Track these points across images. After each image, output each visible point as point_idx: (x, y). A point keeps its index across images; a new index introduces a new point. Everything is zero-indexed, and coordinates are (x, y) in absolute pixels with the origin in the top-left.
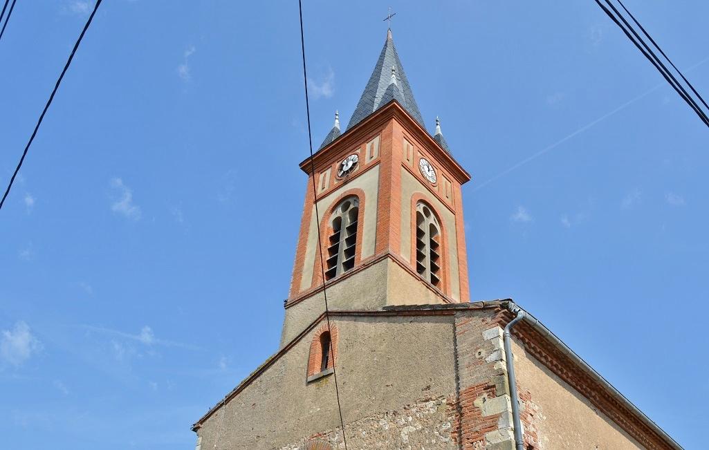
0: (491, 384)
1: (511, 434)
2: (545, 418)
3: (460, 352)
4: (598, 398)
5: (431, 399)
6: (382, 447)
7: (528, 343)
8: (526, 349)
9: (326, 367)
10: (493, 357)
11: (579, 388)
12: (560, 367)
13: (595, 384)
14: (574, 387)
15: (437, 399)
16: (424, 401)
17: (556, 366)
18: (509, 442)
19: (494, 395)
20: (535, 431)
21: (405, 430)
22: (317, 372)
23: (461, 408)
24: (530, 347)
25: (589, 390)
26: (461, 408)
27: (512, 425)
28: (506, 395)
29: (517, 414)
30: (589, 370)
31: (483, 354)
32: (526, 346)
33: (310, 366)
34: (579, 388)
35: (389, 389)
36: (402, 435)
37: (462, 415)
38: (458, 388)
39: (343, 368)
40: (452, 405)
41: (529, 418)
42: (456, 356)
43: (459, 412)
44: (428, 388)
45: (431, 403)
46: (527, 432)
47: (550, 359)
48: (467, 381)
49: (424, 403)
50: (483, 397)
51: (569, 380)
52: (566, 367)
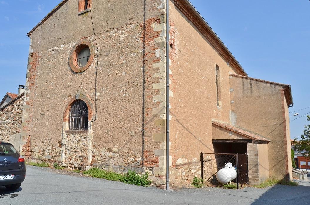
0: (159, 18)
1: (165, 39)
2: (179, 34)
3: (146, 3)
4: (201, 28)
5: (133, 23)
6: (111, 43)
7: (176, 2)
8: (175, 4)
9: (87, 8)
10: (161, 6)
11: (194, 23)
12: (188, 13)
13: (201, 22)
14: (192, 23)
15: (135, 24)
16: (130, 24)
17: (186, 13)
18: (164, 42)
19: (159, 23)
20: (174, 38)
21: (121, 36)
22: (83, 10)
23: (145, 28)
24: (177, 3)
25: (198, 24)
26: (145, 28)
27: (165, 35)
28: (164, 23)
29: (168, 32)
30: (199, 16)
31: (157, 5)
32: (175, 3)
33: (79, 7)
34: (194, 23)
35: (115, 18)
36: (120, 38)
37: (145, 30)
38: (145, 19)
39: (94, 9)
40: (142, 26)
41: (173, 33)
42: (145, 5)
43: (144, 29)
44: (132, 18)
45: (133, 25)
46: (171, 39)
47: (184, 10)
48: (149, 16)
49: (130, 25)
50: (155, 23)
51: (191, 19)
52: (191, 14)
